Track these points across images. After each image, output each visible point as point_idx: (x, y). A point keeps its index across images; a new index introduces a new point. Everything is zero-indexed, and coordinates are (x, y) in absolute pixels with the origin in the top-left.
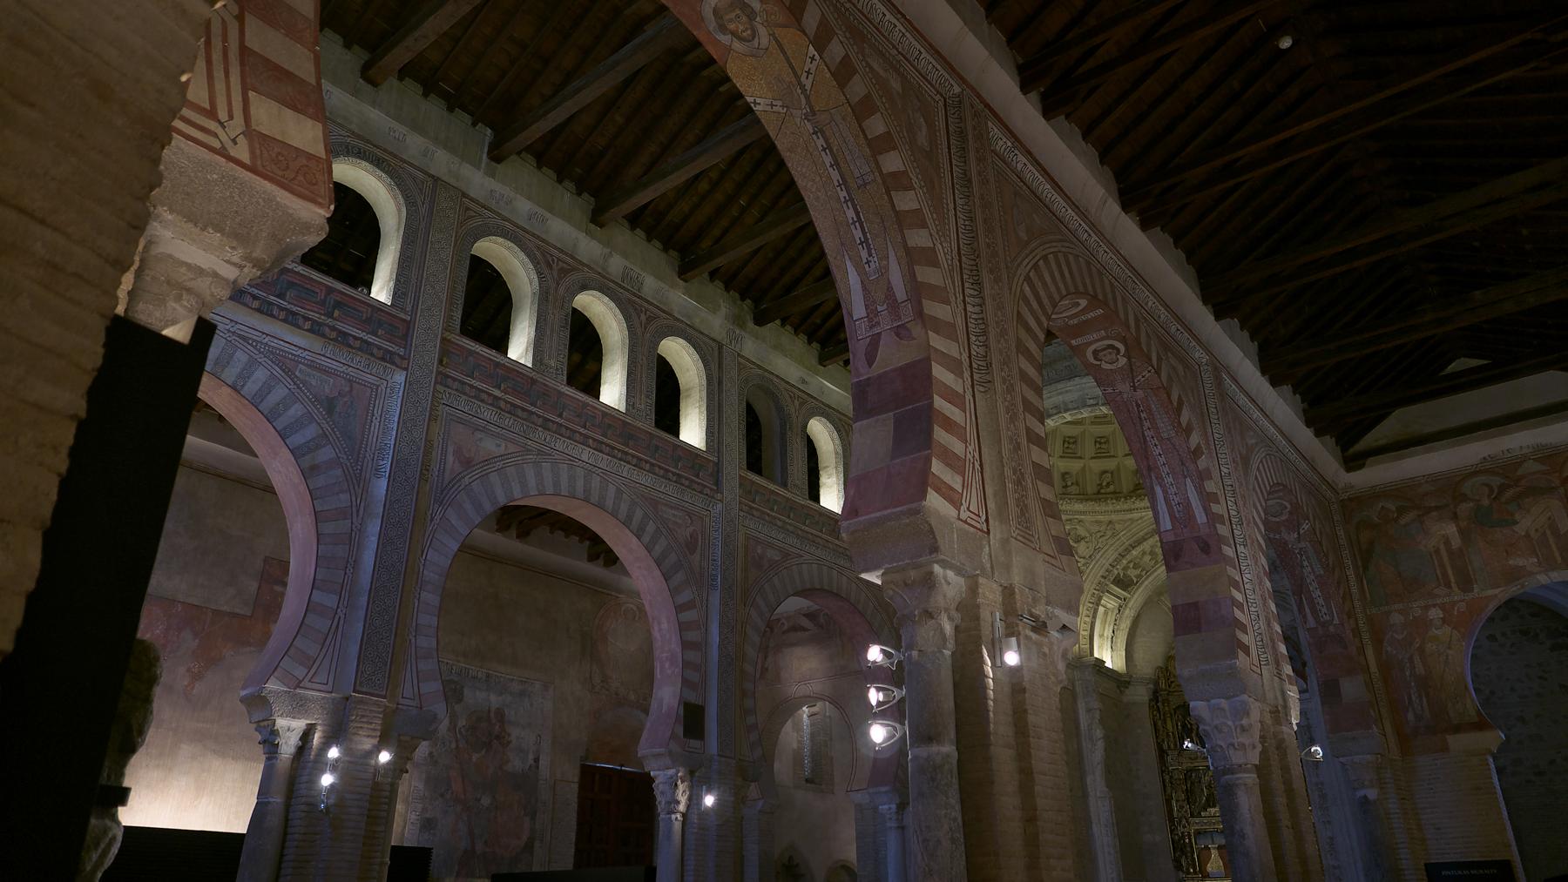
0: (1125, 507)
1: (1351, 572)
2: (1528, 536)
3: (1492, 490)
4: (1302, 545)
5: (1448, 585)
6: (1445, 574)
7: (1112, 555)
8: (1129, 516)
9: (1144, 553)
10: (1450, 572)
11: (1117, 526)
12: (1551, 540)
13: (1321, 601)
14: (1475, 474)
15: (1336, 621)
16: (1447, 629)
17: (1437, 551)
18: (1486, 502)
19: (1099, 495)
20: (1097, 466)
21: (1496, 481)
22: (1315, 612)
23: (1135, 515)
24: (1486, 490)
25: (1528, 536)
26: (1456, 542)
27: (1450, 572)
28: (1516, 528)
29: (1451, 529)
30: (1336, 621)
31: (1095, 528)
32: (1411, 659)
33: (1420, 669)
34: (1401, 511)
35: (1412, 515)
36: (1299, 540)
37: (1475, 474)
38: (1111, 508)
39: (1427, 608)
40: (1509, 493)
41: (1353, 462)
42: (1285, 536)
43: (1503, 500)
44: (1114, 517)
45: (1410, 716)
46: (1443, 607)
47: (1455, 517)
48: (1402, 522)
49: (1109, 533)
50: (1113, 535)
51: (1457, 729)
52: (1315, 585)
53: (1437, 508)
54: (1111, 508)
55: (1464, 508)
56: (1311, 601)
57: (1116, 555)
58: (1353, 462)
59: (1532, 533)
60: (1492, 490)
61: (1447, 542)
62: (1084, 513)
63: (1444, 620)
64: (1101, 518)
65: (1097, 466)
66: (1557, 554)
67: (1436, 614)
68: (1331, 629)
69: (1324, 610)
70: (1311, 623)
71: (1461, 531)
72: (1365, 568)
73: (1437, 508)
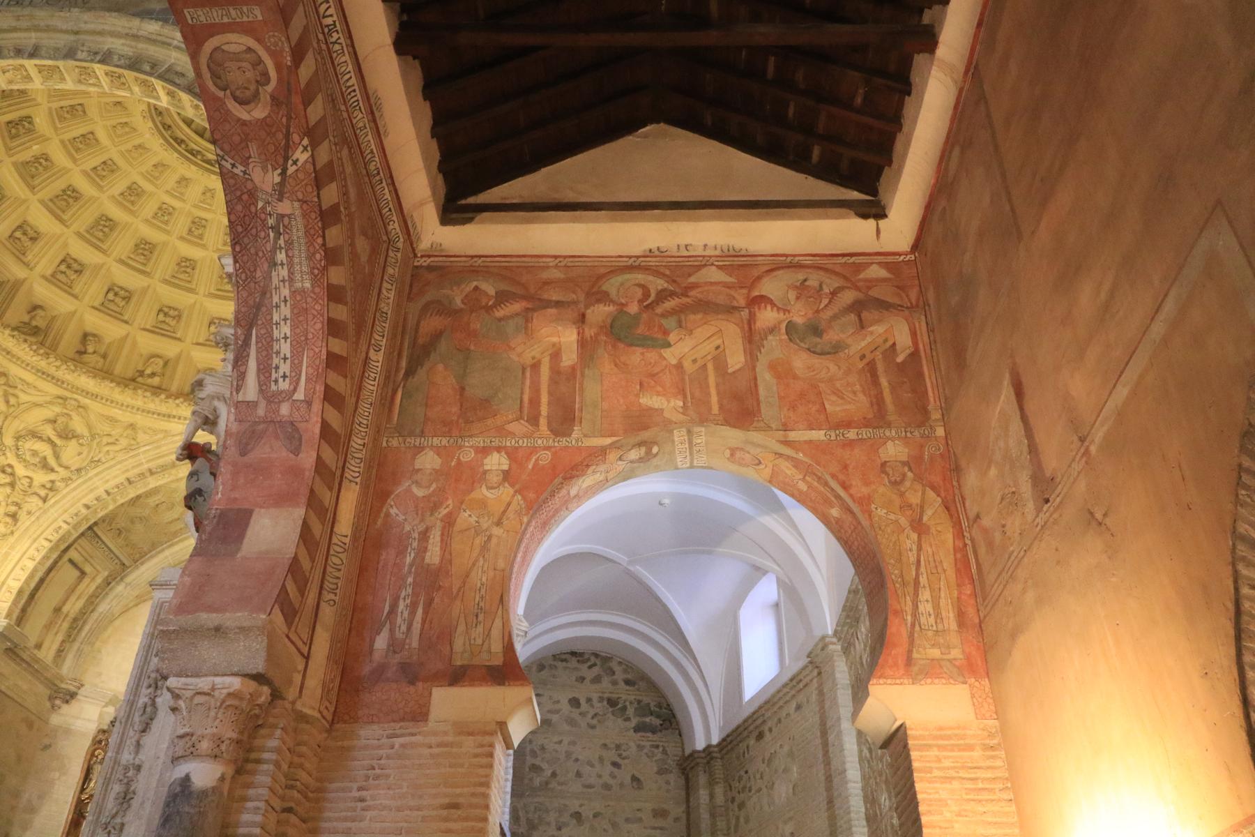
0: (163, 409)
1: (378, 358)
2: (679, 366)
3: (646, 294)
4: (285, 207)
5: (534, 420)
6: (535, 402)
10: (544, 399)
11: (141, 437)
12: (712, 380)
13: (286, 348)
14: (631, 269)
15: (300, 395)
16: (507, 491)
17: (536, 366)
18: (633, 308)
19: (131, 381)
20: (148, 343)
21: (661, 284)
22: (265, 370)
24: (639, 293)
25: (679, 366)
26: (570, 358)
27: (544, 399)
28: (667, 353)
29: (568, 337)
30: (300, 395)
32: (424, 536)
33: (433, 555)
34: (503, 298)
35: (517, 307)
38: (139, 403)
39: (485, 451)
40: (670, 304)
41: (454, 209)
42: (257, 174)
43: (659, 310)
44: (139, 419)
45: (381, 642)
46: (512, 454)
48: (499, 313)
49: (124, 442)
50: (128, 449)
51: (457, 676)
52: (286, 311)
53: (558, 304)
54: (139, 403)
56: (267, 346)
57: (122, 479)
58: (454, 209)
59: (687, 364)
60: (646, 294)
61: (556, 355)
62: (95, 396)
63: (506, 475)
64: (116, 412)
65: (148, 343)
66: (714, 399)
67: (496, 462)
68: (285, 409)
69: (285, 368)
70: (251, 390)
71: (582, 343)
72: (410, 373)
73: (558, 304)
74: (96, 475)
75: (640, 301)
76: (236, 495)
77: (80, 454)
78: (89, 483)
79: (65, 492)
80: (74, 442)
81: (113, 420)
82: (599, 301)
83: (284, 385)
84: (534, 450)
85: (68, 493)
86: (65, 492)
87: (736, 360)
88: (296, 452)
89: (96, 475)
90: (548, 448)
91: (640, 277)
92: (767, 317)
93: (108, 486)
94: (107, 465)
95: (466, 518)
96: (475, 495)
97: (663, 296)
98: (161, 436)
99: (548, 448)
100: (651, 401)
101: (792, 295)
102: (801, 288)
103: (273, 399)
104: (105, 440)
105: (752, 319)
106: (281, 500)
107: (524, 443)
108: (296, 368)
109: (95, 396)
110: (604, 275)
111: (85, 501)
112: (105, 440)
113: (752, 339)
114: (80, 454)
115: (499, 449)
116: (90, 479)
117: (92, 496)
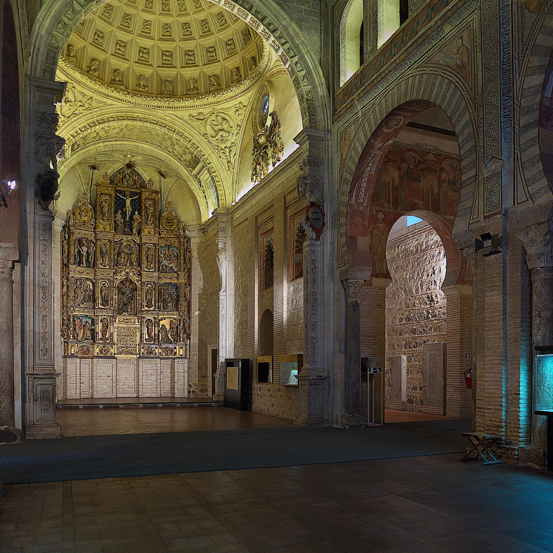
0: (106, 91)
6: (389, 197)
7: (82, 122)
8: (105, 100)
9: (95, 132)
13: (363, 190)
14: (411, 150)
15: (365, 204)
17: (389, 183)
21: (418, 158)
23: (109, 102)
25: (423, 190)
26: (397, 182)
29: (396, 174)
30: (365, 204)
31: (80, 97)
36: (379, 149)
37: (411, 150)
38: (97, 87)
39: (378, 211)
44: (95, 96)
47: (400, 168)
49: (87, 105)
52: (366, 179)
55: (404, 166)
57: (85, 124)
61: (393, 181)
62: (78, 82)
64: (86, 92)
67: (381, 215)
69: (362, 196)
70: (353, 201)
71: (400, 177)
74: (75, 120)
75: (414, 164)
76: (352, 231)
77: (70, 109)
78: (73, 124)
79: (63, 128)
80: (68, 103)
81: (84, 95)
82: (403, 162)
83: (362, 201)
84: (389, 213)
85: (65, 128)
86: (63, 128)
87: (436, 190)
88: (364, 221)
89: (75, 120)
90: (393, 213)
91: (413, 154)
92: (444, 176)
93: (80, 126)
94: (79, 116)
95: (375, 232)
96: (376, 225)
97: (420, 162)
98: (102, 104)
99: (393, 213)
100: (417, 201)
101: (450, 169)
102: (452, 166)
103: (359, 204)
104: (80, 104)
105: (440, 176)
106: (363, 234)
107: (387, 210)
108: (365, 196)
109: (78, 82)
110: (404, 151)
111: (71, 133)
112: (80, 104)
113: (440, 183)
114: (70, 109)
115: (381, 211)
116: (73, 122)
117: (73, 131)
